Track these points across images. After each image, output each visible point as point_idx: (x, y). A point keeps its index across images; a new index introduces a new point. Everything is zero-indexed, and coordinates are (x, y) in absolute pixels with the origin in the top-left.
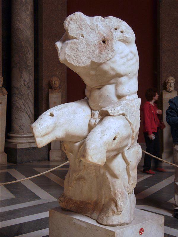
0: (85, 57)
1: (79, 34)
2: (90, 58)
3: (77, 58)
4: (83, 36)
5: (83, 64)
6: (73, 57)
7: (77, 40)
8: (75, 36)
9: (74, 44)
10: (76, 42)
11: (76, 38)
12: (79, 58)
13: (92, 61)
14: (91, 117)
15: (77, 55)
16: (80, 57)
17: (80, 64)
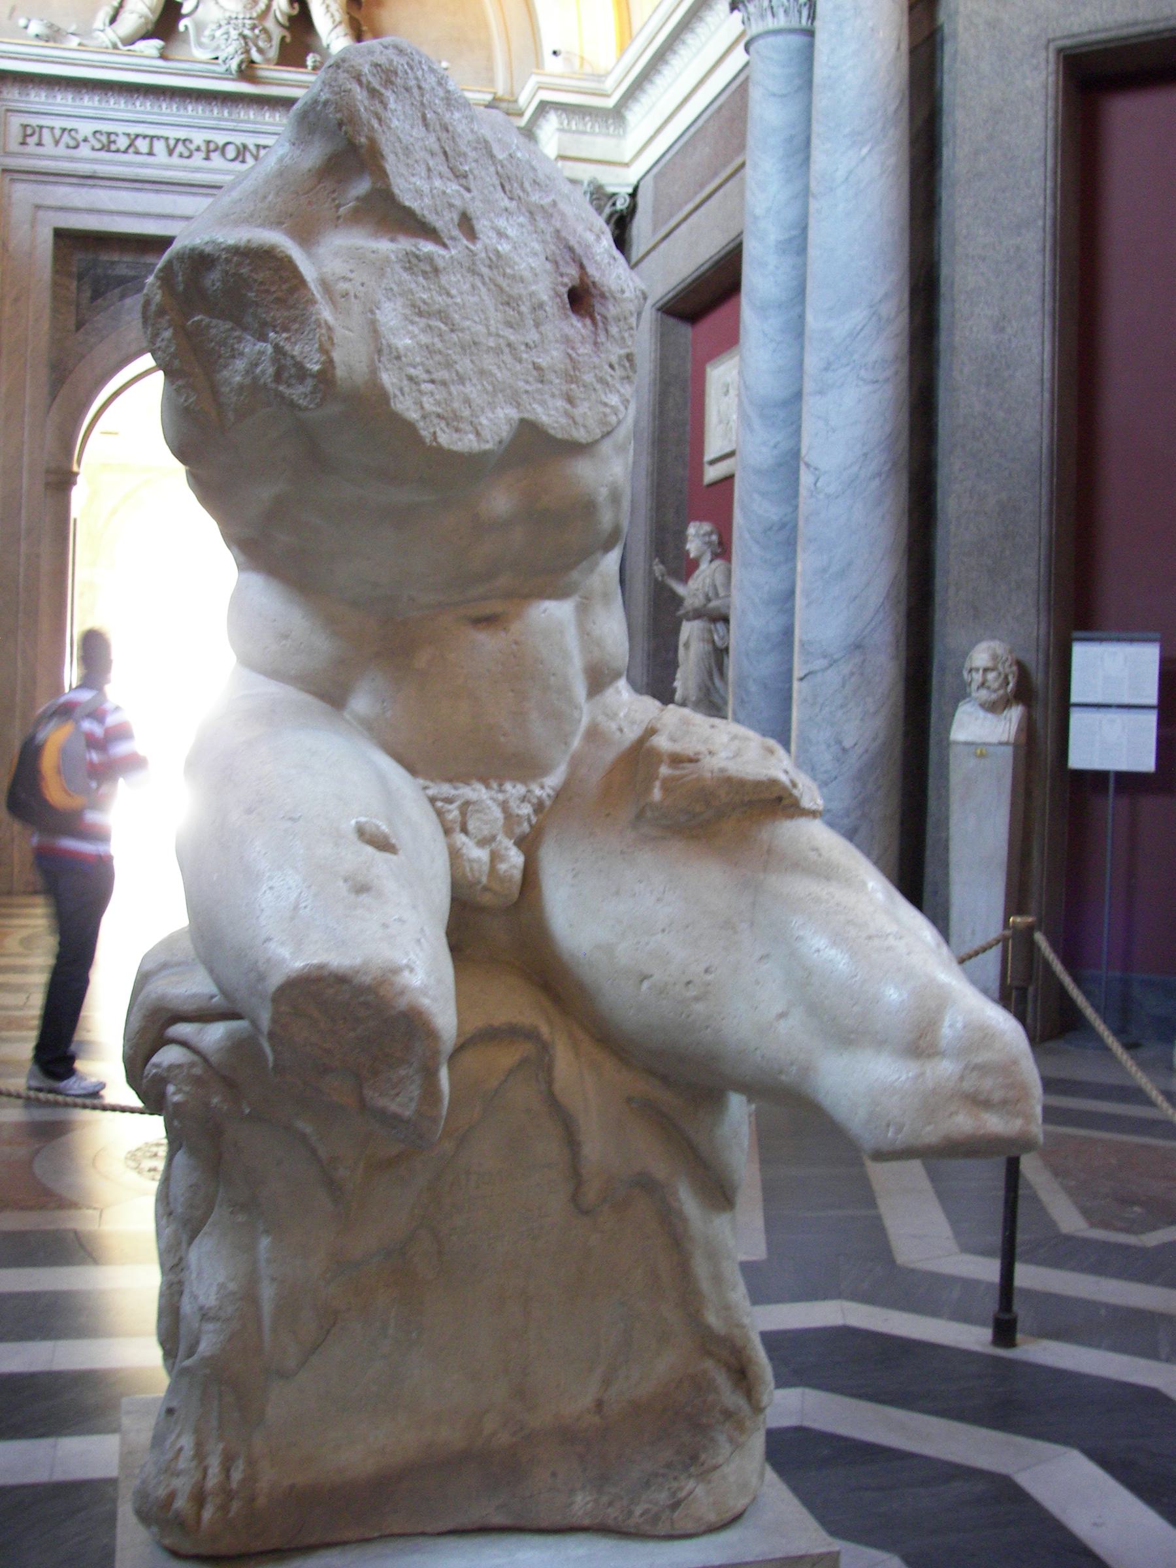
0: (490, 388)
1: (451, 206)
2: (515, 399)
3: (444, 383)
4: (466, 224)
5: (478, 434)
6: (418, 372)
7: (442, 252)
8: (431, 218)
9: (424, 273)
10: (441, 264)
11: (429, 232)
12: (452, 388)
13: (523, 421)
14: (447, 832)
15: (449, 365)
16: (461, 380)
17: (457, 430)
